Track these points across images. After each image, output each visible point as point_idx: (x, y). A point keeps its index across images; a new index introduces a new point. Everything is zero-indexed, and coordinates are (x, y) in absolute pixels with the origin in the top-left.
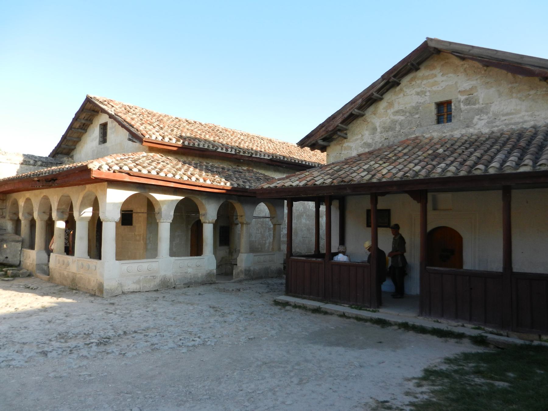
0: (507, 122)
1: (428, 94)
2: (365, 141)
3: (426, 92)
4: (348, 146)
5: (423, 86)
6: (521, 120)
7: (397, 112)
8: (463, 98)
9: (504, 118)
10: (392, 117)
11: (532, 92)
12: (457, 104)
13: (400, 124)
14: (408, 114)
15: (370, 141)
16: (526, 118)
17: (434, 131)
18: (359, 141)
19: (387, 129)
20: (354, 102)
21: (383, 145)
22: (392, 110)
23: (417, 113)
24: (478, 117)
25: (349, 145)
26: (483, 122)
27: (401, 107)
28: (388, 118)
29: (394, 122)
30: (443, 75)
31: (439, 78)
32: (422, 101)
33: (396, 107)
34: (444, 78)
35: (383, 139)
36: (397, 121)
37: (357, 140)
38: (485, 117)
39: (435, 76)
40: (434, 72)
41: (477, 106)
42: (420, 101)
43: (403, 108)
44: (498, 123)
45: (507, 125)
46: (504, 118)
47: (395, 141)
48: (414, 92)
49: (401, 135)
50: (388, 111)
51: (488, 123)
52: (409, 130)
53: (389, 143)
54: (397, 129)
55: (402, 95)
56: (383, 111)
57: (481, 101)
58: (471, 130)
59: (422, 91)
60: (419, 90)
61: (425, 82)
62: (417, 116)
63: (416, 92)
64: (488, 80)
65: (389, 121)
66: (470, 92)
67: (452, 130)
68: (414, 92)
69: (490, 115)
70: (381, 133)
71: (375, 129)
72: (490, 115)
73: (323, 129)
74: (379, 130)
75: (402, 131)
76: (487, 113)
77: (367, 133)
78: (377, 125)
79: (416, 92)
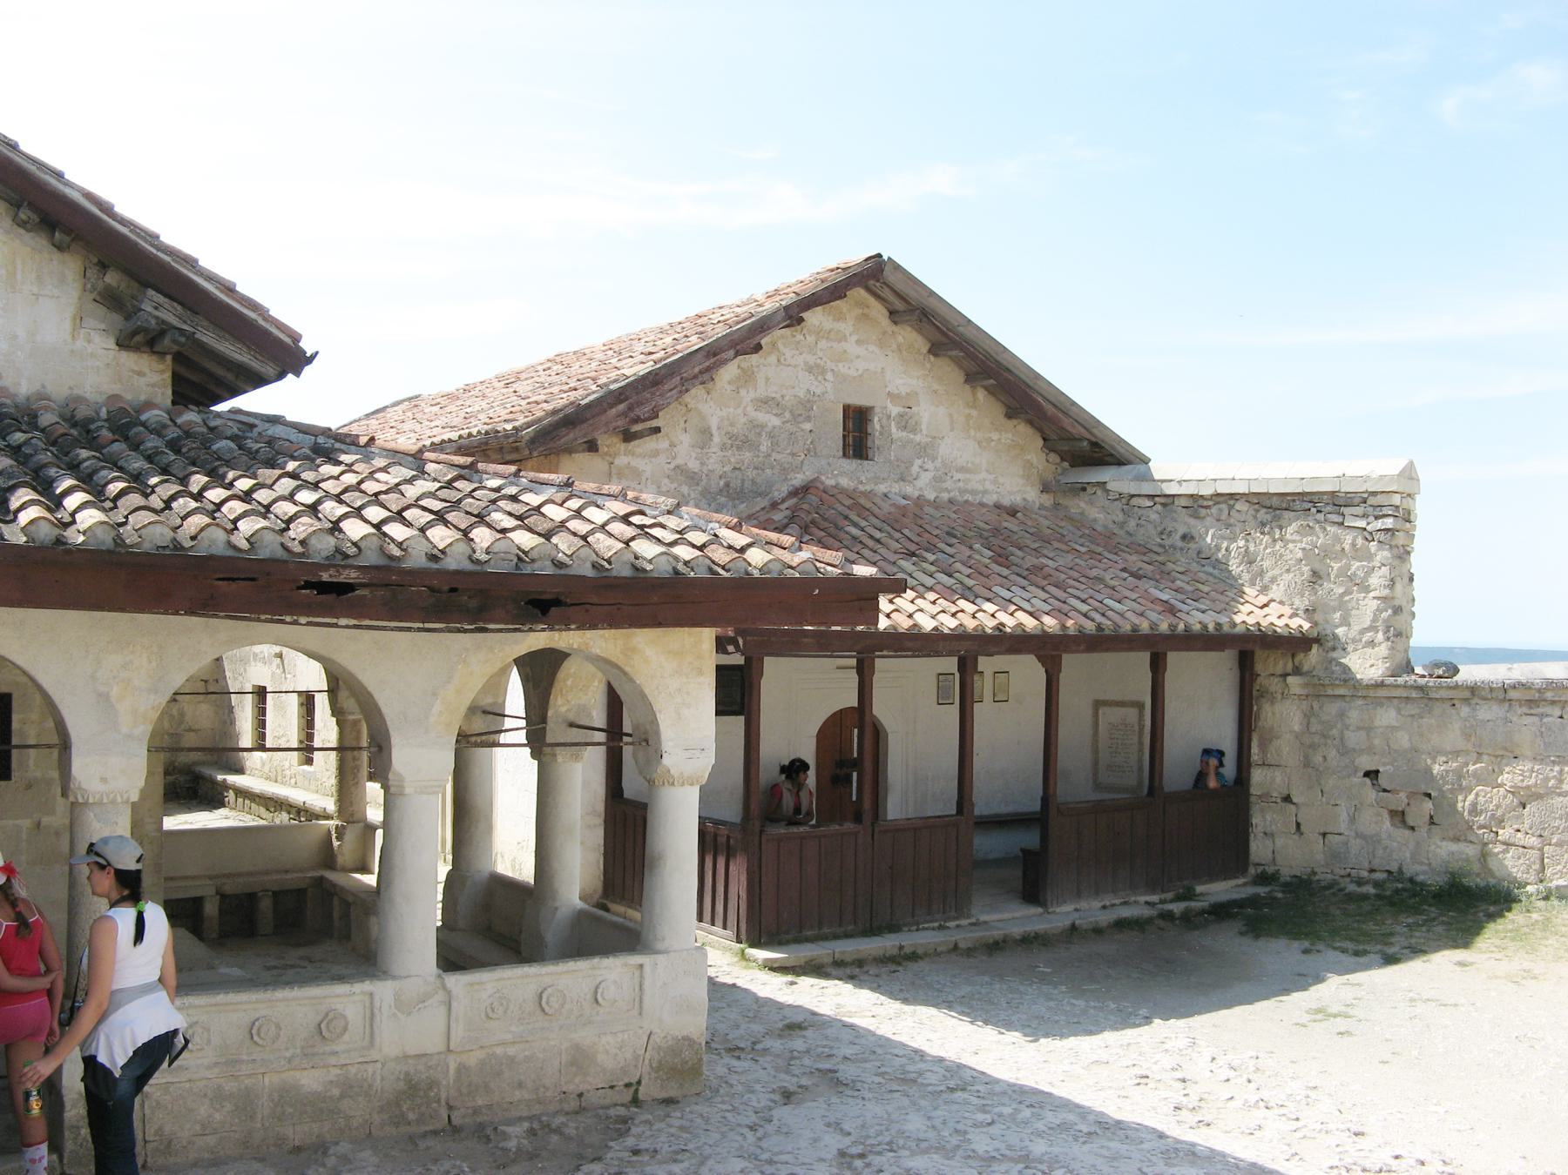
0: (961, 484)
1: (829, 376)
2: (679, 461)
3: (824, 372)
4: (628, 466)
5: (820, 354)
6: (980, 488)
7: (764, 403)
8: (895, 410)
9: (958, 476)
10: (753, 414)
11: (995, 436)
12: (884, 421)
13: (771, 436)
14: (787, 415)
15: (693, 465)
16: (989, 486)
17: (842, 474)
18: (662, 459)
19: (740, 442)
20: (715, 355)
21: (727, 485)
22: (752, 395)
23: (808, 419)
24: (918, 462)
25: (633, 463)
26: (929, 475)
27: (773, 391)
28: (740, 411)
29: (757, 427)
30: (858, 342)
31: (851, 347)
32: (818, 392)
33: (762, 392)
34: (860, 351)
35: (728, 468)
36: (762, 426)
37: (656, 453)
38: (929, 465)
39: (844, 339)
40: (841, 326)
41: (918, 438)
42: (813, 389)
43: (778, 396)
44: (948, 484)
45: (962, 491)
46: (958, 476)
47: (759, 480)
48: (800, 360)
49: (772, 468)
50: (743, 392)
51: (935, 478)
52: (790, 459)
53: (743, 481)
54: (763, 448)
55: (773, 359)
56: (729, 388)
57: (924, 427)
58: (909, 490)
59: (818, 366)
60: (811, 359)
61: (823, 344)
62: (807, 426)
63: (806, 363)
64: (936, 386)
65: (743, 420)
66: (907, 402)
67: (877, 480)
68: (800, 360)
69: (938, 463)
70: (723, 448)
71: (706, 433)
72: (938, 463)
73: (621, 407)
74: (716, 439)
75: (774, 455)
76: (934, 459)
77: (685, 440)
78: (714, 423)
79: (806, 363)
